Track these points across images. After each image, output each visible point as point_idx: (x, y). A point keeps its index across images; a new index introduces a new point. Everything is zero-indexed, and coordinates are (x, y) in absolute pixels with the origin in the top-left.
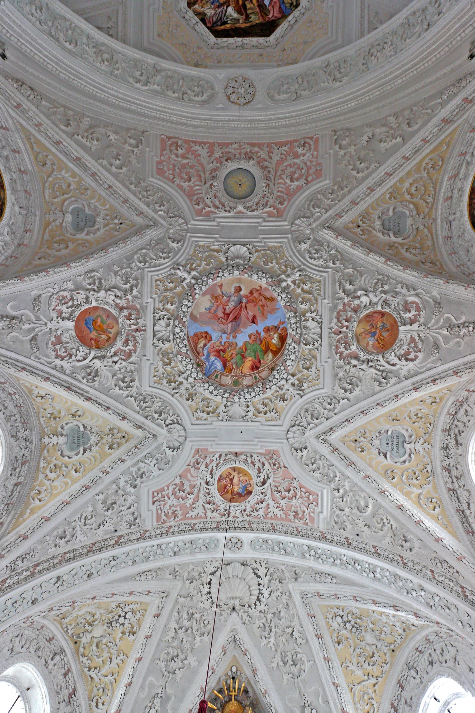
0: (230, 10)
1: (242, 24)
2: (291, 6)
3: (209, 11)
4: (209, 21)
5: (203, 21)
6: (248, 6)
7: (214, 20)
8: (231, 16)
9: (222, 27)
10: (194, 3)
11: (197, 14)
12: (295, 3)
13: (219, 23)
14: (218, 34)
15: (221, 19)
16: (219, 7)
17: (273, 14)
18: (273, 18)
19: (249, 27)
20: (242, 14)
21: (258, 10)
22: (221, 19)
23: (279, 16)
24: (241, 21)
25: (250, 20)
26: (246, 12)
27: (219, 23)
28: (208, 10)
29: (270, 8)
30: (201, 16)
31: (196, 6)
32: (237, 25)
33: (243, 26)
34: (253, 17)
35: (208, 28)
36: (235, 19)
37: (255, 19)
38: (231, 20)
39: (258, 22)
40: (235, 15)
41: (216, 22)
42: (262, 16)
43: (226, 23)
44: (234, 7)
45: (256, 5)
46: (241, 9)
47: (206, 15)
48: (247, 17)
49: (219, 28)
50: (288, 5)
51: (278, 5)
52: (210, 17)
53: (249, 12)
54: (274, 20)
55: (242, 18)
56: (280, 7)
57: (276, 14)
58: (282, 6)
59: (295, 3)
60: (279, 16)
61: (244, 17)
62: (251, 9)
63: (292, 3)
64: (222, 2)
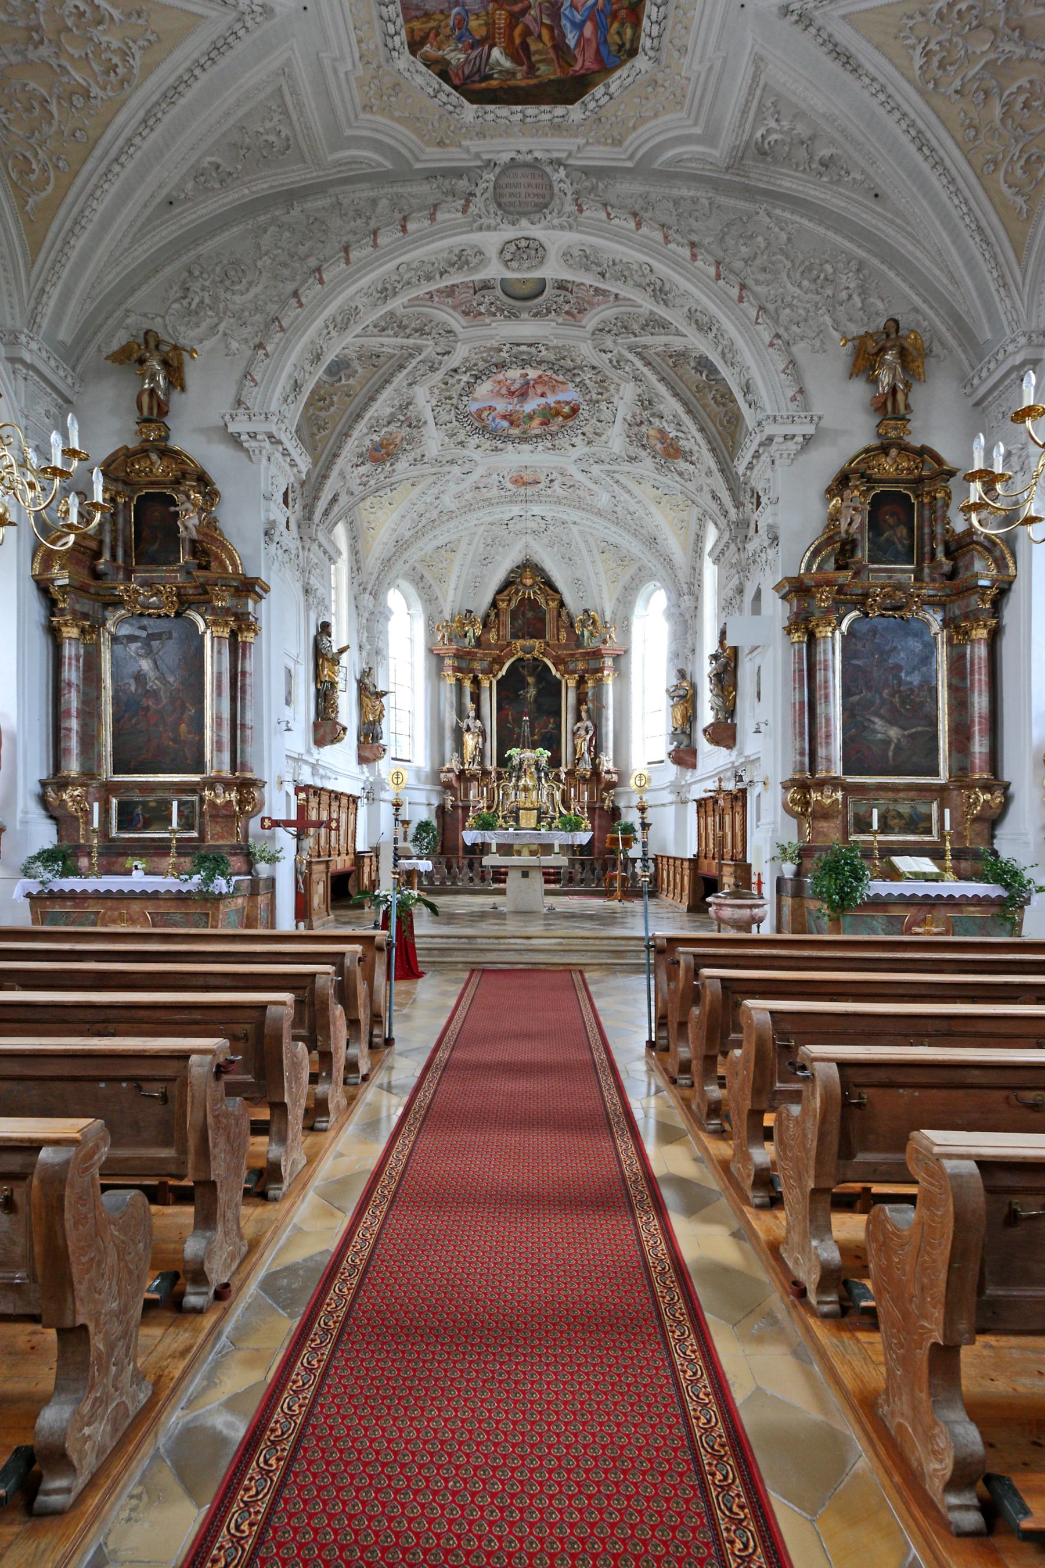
0: (496, 53)
1: (520, 80)
2: (619, 51)
3: (456, 57)
4: (457, 74)
5: (444, 75)
6: (533, 47)
7: (466, 72)
8: (498, 63)
9: (483, 85)
10: (423, 42)
11: (430, 63)
12: (628, 46)
13: (476, 78)
14: (477, 97)
15: (479, 70)
16: (472, 47)
17: (582, 63)
18: (583, 71)
19: (535, 86)
20: (521, 64)
21: (552, 55)
22: (479, 70)
23: (595, 67)
24: (519, 76)
25: (538, 73)
26: (529, 58)
27: (476, 78)
28: (453, 54)
29: (576, 52)
30: (439, 67)
31: (427, 48)
32: (512, 83)
33: (523, 83)
34: (543, 69)
35: (455, 87)
36: (508, 72)
37: (547, 71)
38: (500, 72)
39: (552, 77)
40: (507, 64)
41: (468, 77)
42: (560, 66)
43: (490, 77)
44: (505, 48)
45: (549, 44)
46: (520, 53)
47: (448, 63)
48: (532, 68)
49: (477, 86)
50: (614, 48)
51: (594, 45)
52: (457, 67)
53: (534, 58)
54: (583, 76)
55: (521, 71)
56: (598, 51)
57: (588, 64)
58: (602, 49)
59: (628, 46)
60: (595, 67)
61: (525, 68)
62: (538, 52)
63: (623, 44)
64: (478, 37)
